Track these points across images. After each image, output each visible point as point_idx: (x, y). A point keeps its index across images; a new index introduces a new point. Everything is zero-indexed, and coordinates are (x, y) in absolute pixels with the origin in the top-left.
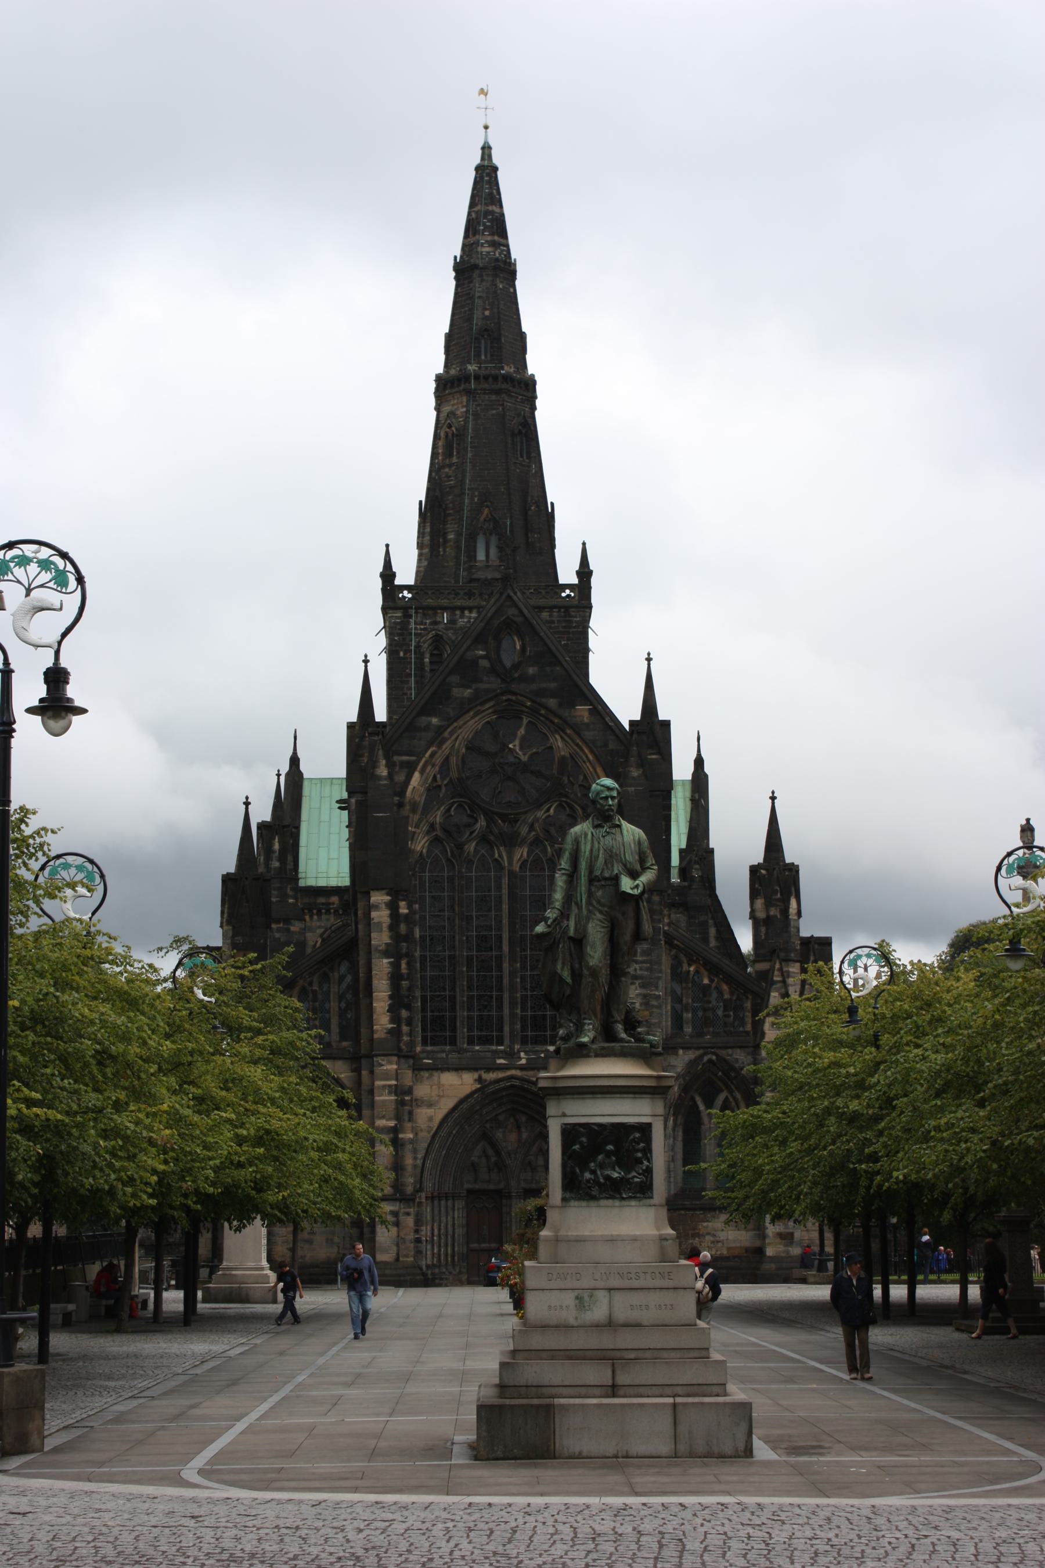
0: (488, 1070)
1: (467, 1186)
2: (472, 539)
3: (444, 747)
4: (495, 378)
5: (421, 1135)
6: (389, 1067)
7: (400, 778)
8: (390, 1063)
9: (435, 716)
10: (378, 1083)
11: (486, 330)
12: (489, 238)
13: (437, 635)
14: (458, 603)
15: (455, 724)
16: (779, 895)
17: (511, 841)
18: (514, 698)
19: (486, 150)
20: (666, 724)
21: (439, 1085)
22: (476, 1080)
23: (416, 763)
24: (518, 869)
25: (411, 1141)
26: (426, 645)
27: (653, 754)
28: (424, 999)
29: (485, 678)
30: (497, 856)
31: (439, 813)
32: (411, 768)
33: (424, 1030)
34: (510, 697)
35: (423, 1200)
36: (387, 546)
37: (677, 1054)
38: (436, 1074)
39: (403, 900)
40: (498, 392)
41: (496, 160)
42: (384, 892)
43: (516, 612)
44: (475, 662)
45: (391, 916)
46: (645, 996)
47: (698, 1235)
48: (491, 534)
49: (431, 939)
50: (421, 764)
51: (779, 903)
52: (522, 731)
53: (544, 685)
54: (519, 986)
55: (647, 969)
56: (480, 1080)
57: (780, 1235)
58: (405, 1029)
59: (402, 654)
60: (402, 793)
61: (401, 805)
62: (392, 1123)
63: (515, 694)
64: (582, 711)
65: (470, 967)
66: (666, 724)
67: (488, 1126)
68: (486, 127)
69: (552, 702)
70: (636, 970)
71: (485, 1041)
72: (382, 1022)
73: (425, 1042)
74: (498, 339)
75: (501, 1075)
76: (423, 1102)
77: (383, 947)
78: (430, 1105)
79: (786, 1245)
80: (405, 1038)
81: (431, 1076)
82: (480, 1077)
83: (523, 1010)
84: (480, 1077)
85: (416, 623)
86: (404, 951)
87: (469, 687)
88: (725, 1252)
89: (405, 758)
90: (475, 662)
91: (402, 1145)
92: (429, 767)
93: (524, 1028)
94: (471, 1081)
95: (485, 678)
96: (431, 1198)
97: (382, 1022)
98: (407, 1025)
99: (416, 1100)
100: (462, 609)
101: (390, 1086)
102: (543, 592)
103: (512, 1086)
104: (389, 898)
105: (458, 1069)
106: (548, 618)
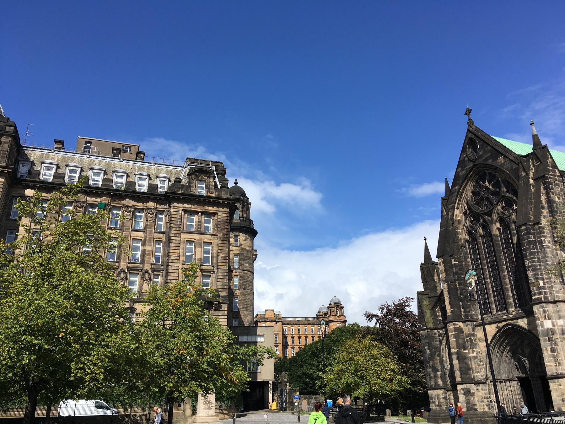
0: (499, 322)
3: (463, 196)
8: (451, 325)
9: (457, 186)
10: (450, 334)
18: (478, 167)
22: (496, 327)
24: (498, 233)
25: (474, 357)
27: (537, 163)
29: (468, 164)
31: (467, 221)
43: (471, 134)
44: (464, 160)
45: (444, 266)
53: (486, 156)
54: (508, 283)
56: (497, 327)
58: (462, 310)
60: (452, 219)
61: (453, 223)
62: (456, 350)
64: (501, 159)
65: (490, 279)
69: (490, 162)
70: (528, 263)
76: (481, 340)
77: (444, 279)
80: (463, 314)
82: (497, 325)
84: (497, 325)
86: (456, 278)
87: (464, 170)
89: (452, 205)
90: (464, 160)
92: (461, 205)
93: (514, 301)
94: (495, 328)
95: (468, 164)
99: (479, 339)
101: (453, 334)
104: (443, 259)
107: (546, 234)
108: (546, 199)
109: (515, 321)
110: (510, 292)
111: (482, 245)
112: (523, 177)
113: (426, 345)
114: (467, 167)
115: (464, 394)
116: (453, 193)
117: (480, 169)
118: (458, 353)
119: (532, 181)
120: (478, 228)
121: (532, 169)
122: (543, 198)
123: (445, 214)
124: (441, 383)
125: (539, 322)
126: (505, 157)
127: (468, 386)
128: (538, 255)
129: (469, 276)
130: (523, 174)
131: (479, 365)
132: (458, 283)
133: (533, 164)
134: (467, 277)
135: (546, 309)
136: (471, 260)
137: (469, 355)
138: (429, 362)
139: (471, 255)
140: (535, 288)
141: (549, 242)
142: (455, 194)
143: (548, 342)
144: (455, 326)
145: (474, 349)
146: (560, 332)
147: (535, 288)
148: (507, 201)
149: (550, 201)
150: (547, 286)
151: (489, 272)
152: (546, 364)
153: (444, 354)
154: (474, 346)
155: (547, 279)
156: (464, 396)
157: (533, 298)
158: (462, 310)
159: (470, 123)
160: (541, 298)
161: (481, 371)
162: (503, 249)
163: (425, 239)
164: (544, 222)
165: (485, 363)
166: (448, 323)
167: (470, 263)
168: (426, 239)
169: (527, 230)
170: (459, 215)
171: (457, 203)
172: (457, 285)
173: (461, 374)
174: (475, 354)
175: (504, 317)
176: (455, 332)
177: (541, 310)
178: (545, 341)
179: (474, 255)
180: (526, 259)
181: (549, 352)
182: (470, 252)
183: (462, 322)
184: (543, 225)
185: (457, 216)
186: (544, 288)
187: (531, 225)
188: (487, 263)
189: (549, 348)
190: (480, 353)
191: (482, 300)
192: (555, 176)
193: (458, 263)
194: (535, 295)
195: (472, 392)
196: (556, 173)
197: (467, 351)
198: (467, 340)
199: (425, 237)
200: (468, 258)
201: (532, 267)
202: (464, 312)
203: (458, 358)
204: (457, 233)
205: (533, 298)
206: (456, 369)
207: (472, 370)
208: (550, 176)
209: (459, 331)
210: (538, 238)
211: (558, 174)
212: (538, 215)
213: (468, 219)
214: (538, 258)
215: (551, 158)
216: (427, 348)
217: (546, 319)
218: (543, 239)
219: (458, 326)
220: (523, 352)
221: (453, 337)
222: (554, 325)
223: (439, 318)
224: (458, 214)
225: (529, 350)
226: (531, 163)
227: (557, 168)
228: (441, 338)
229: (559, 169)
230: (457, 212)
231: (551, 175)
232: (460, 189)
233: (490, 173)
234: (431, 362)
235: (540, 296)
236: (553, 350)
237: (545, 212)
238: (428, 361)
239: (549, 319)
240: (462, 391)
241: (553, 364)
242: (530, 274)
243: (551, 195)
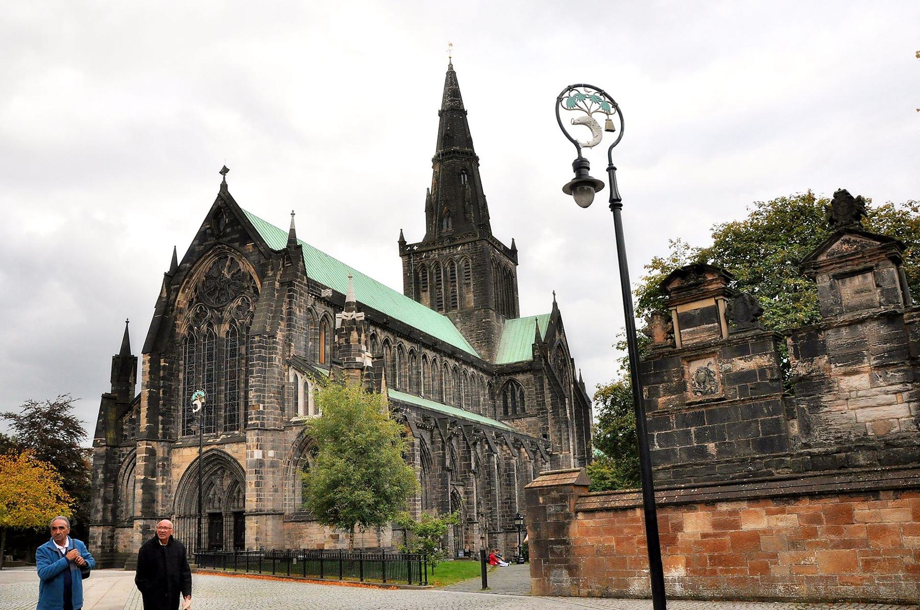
1: (208, 511)
2: (441, 221)
3: (194, 278)
4: (450, 153)
5: (174, 483)
6: (143, 447)
7: (172, 297)
10: (138, 456)
11: (447, 135)
12: (450, 99)
13: (422, 264)
14: (429, 248)
15: (197, 265)
16: (345, 332)
17: (220, 321)
18: (220, 246)
19: (451, 66)
20: (300, 246)
21: (182, 456)
23: (180, 287)
24: (224, 336)
25: (163, 487)
26: (419, 269)
28: (184, 411)
30: (215, 330)
31: (191, 312)
32: (177, 291)
33: (183, 427)
34: (219, 246)
35: (175, 519)
36: (401, 230)
37: (292, 429)
38: (180, 449)
39: (162, 358)
40: (451, 158)
41: (455, 69)
42: (148, 354)
46: (257, 396)
47: (301, 537)
48: (448, 218)
49: (188, 379)
50: (182, 288)
51: (344, 336)
52: (228, 263)
53: (233, 237)
54: (223, 399)
55: (259, 381)
56: (200, 452)
57: (331, 536)
58: (161, 426)
59: (408, 275)
60: (173, 305)
61: (172, 311)
62: (143, 477)
63: (221, 244)
64: (250, 245)
66: (300, 246)
67: (213, 477)
68: (450, 58)
71: (209, 431)
72: (144, 423)
73: (183, 435)
74: (452, 137)
75: (209, 448)
77: (146, 383)
78: (178, 467)
79: (334, 543)
80: (161, 431)
81: (179, 451)
83: (225, 412)
85: (413, 260)
88: (316, 547)
91: (157, 489)
92: (187, 290)
93: (225, 423)
95: (209, 239)
96: (179, 518)
97: (144, 423)
98: (161, 424)
100: (431, 250)
101: (143, 457)
102: (464, 236)
103: (214, 455)
104: (150, 357)
105: (190, 447)
106: (467, 248)
107: (278, 351)
108: (287, 309)
109: (221, 446)
110: (223, 411)
111: (202, 347)
112: (269, 277)
113: (100, 468)
114: (207, 243)
115: (142, 533)
116: (182, 271)
117: (221, 250)
118: (145, 480)
119: (277, 284)
120: (203, 324)
121: (280, 270)
122: (285, 308)
123: (165, 295)
124: (110, 518)
125: (250, 451)
126: (255, 246)
127: (148, 522)
128: (265, 374)
129: (196, 396)
130: (270, 273)
131: (166, 496)
132: (163, 391)
133: (283, 263)
134: (194, 397)
135: (260, 437)
136: (185, 364)
137: (157, 484)
138: (100, 490)
139: (185, 357)
140: (253, 412)
141: (279, 361)
142: (183, 273)
143: (254, 475)
144: (148, 446)
145: (165, 477)
146: (269, 464)
147: (253, 412)
148: (244, 300)
149: (290, 313)
150: (266, 411)
151: (203, 382)
152: (246, 499)
153: (120, 480)
154: (166, 472)
155: (268, 403)
156: (141, 535)
157: (249, 423)
158: (161, 426)
159: (224, 186)
160: (258, 425)
161: (167, 504)
162: (227, 358)
163: (127, 322)
164: (280, 336)
165: (174, 495)
166: (138, 441)
167: (182, 368)
168: (129, 322)
169: (260, 342)
170: (182, 302)
171: (183, 285)
172: (161, 393)
173: (143, 507)
174: (164, 483)
175: (209, 441)
176: (146, 454)
177: (255, 438)
178: (251, 473)
179: (190, 357)
180: (251, 377)
181: (253, 486)
182: (185, 353)
183: (157, 441)
184: (277, 340)
185: (180, 303)
186: (262, 413)
187: (265, 338)
188: (204, 372)
189: (254, 482)
190: (170, 482)
191: (187, 417)
192: (302, 284)
193: (167, 365)
194: (251, 419)
195: (151, 530)
196: (304, 280)
197: (155, 479)
198: (158, 464)
199: (128, 319)
200: (182, 360)
201: (256, 387)
202: (163, 429)
203: (142, 488)
204: (175, 325)
205: (249, 423)
206: (137, 501)
207: (157, 502)
208: (297, 283)
209: (152, 453)
210: (270, 353)
211: (305, 282)
212: (275, 327)
213: (192, 310)
214: (264, 378)
215: (303, 261)
216: (100, 471)
217: (257, 448)
218: (274, 356)
219: (151, 447)
220: (222, 483)
221: (142, 461)
222: (264, 456)
223: (125, 433)
224: (181, 299)
225: (229, 482)
226: (281, 262)
227: (306, 274)
228: (122, 460)
229: (308, 276)
230: (181, 296)
231: (299, 282)
232: (191, 268)
233: (232, 259)
234: (102, 491)
235: (258, 422)
236: (258, 484)
237: (283, 324)
238: (99, 488)
239: (260, 449)
240: (139, 528)
241: (255, 499)
242: (252, 394)
243: (294, 307)
